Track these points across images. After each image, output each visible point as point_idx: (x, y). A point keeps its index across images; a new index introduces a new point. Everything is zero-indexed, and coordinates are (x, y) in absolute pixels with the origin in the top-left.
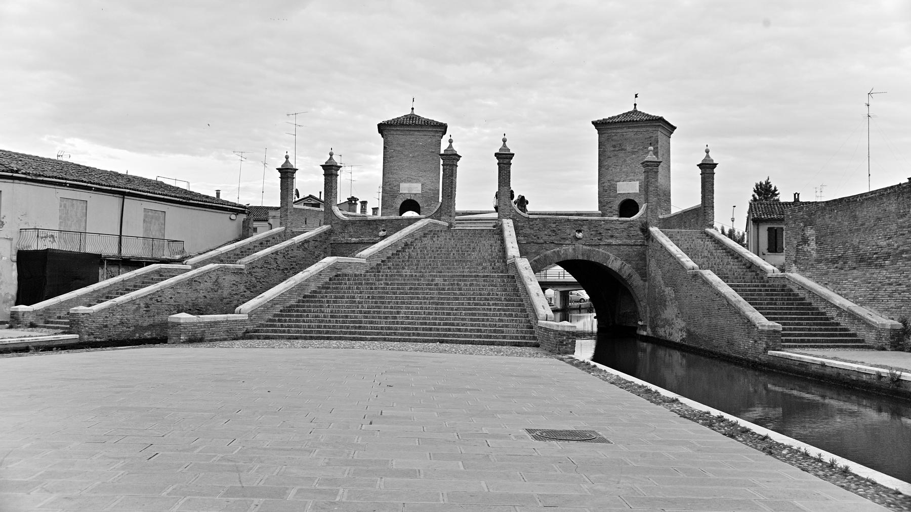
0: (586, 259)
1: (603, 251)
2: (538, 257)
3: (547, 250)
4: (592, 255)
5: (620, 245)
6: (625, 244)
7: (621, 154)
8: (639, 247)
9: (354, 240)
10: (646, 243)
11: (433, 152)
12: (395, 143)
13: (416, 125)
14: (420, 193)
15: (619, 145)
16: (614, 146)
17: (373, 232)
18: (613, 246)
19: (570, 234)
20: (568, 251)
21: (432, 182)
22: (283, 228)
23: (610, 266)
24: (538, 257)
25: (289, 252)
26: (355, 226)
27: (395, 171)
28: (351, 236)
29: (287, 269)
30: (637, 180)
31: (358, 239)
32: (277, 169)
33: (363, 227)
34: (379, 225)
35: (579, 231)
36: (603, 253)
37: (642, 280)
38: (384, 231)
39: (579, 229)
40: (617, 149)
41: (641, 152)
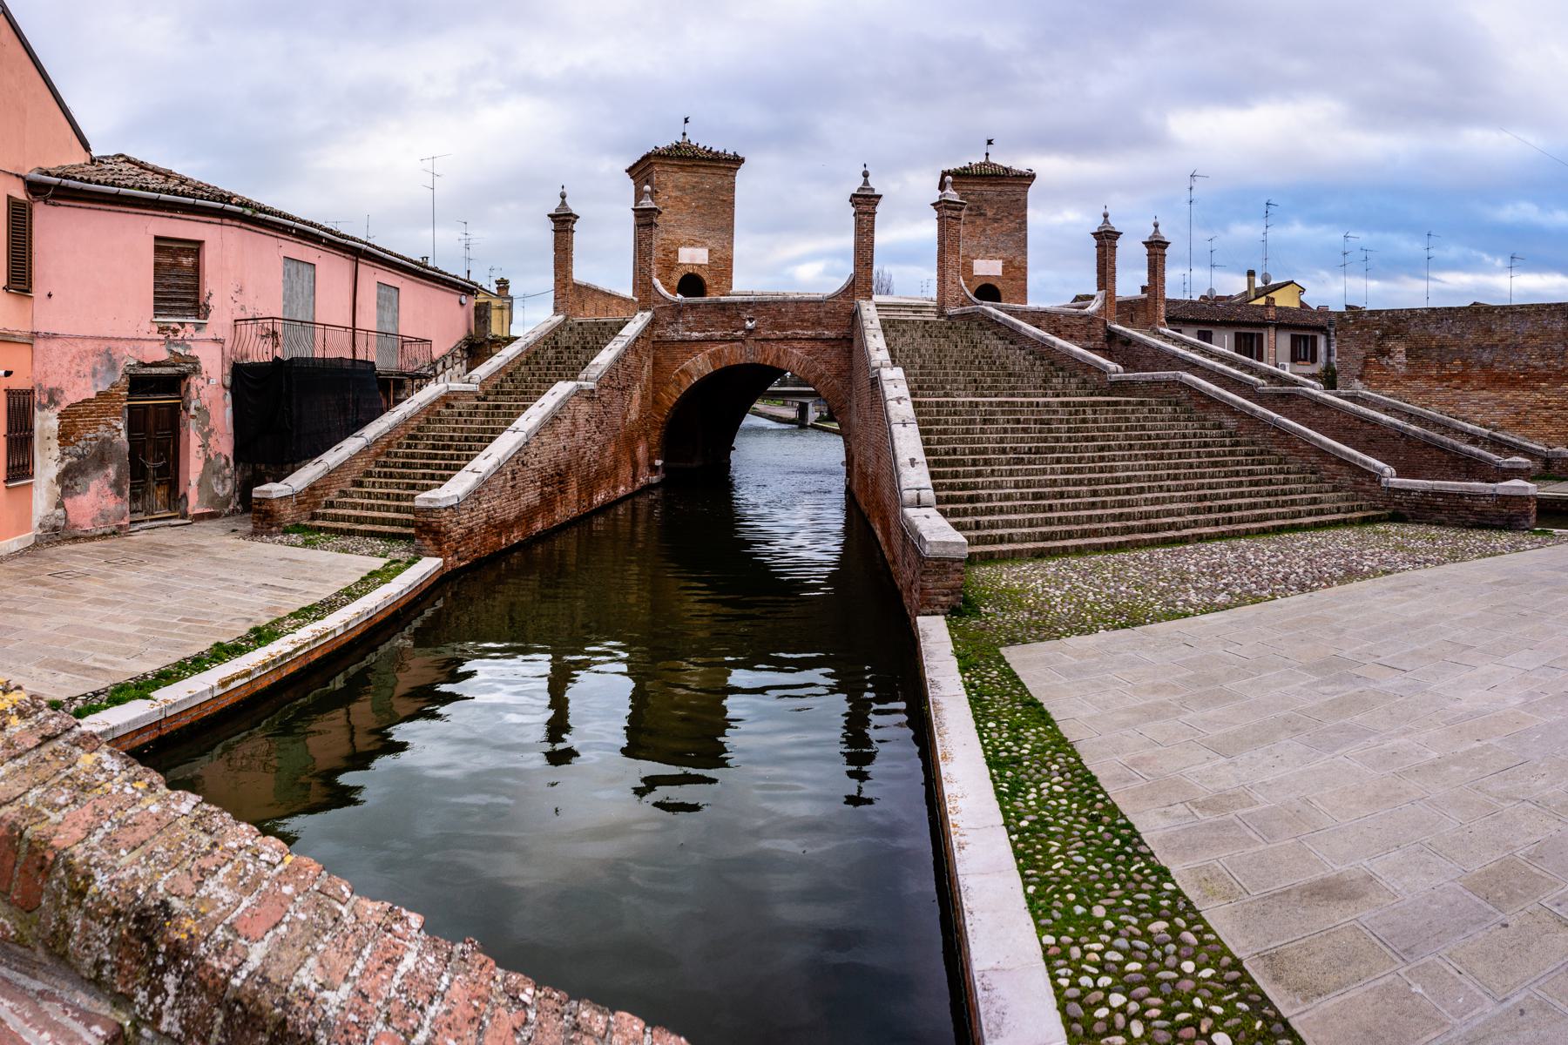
7: (979, 221)
9: (695, 334)
12: (670, 185)
17: (730, 322)
28: (691, 330)
31: (703, 334)
38: (751, 320)
41: (1005, 221)
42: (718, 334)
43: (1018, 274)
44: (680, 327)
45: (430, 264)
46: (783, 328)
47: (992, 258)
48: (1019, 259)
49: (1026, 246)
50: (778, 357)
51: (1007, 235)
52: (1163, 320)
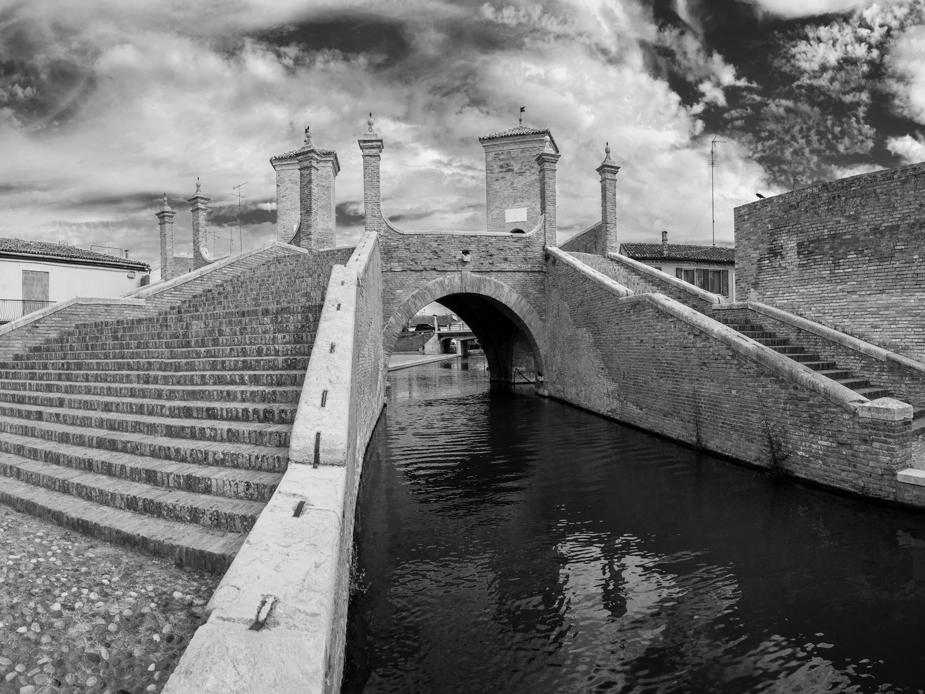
0: (475, 292)
1: (496, 280)
2: (417, 290)
3: (428, 280)
4: (482, 286)
5: (514, 271)
6: (521, 269)
8: (537, 274)
10: (545, 269)
18: (507, 273)
19: (455, 257)
20: (454, 283)
23: (504, 302)
24: (417, 290)
35: (466, 252)
36: (495, 283)
37: (541, 319)
39: (466, 249)
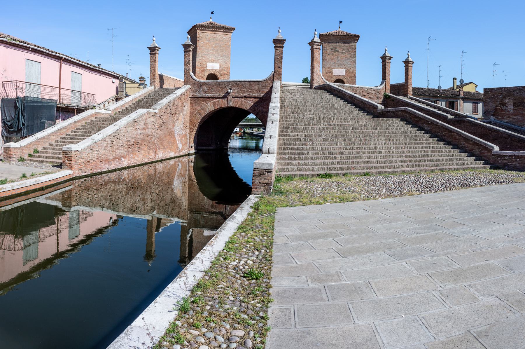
7: (336, 54)
9: (207, 95)
11: (226, 45)
13: (217, 28)
14: (219, 69)
15: (334, 48)
16: (332, 49)
21: (226, 63)
22: (153, 87)
25: (175, 102)
26: (208, 86)
27: (204, 55)
28: (206, 93)
29: (174, 114)
30: (344, 68)
31: (210, 95)
32: (148, 48)
33: (214, 87)
34: (227, 85)
38: (230, 89)
40: (333, 50)
42: (217, 95)
43: (352, 75)
44: (201, 92)
45: (101, 67)
46: (243, 92)
47: (341, 68)
48: (352, 69)
49: (355, 64)
50: (242, 104)
51: (347, 59)
52: (411, 93)
